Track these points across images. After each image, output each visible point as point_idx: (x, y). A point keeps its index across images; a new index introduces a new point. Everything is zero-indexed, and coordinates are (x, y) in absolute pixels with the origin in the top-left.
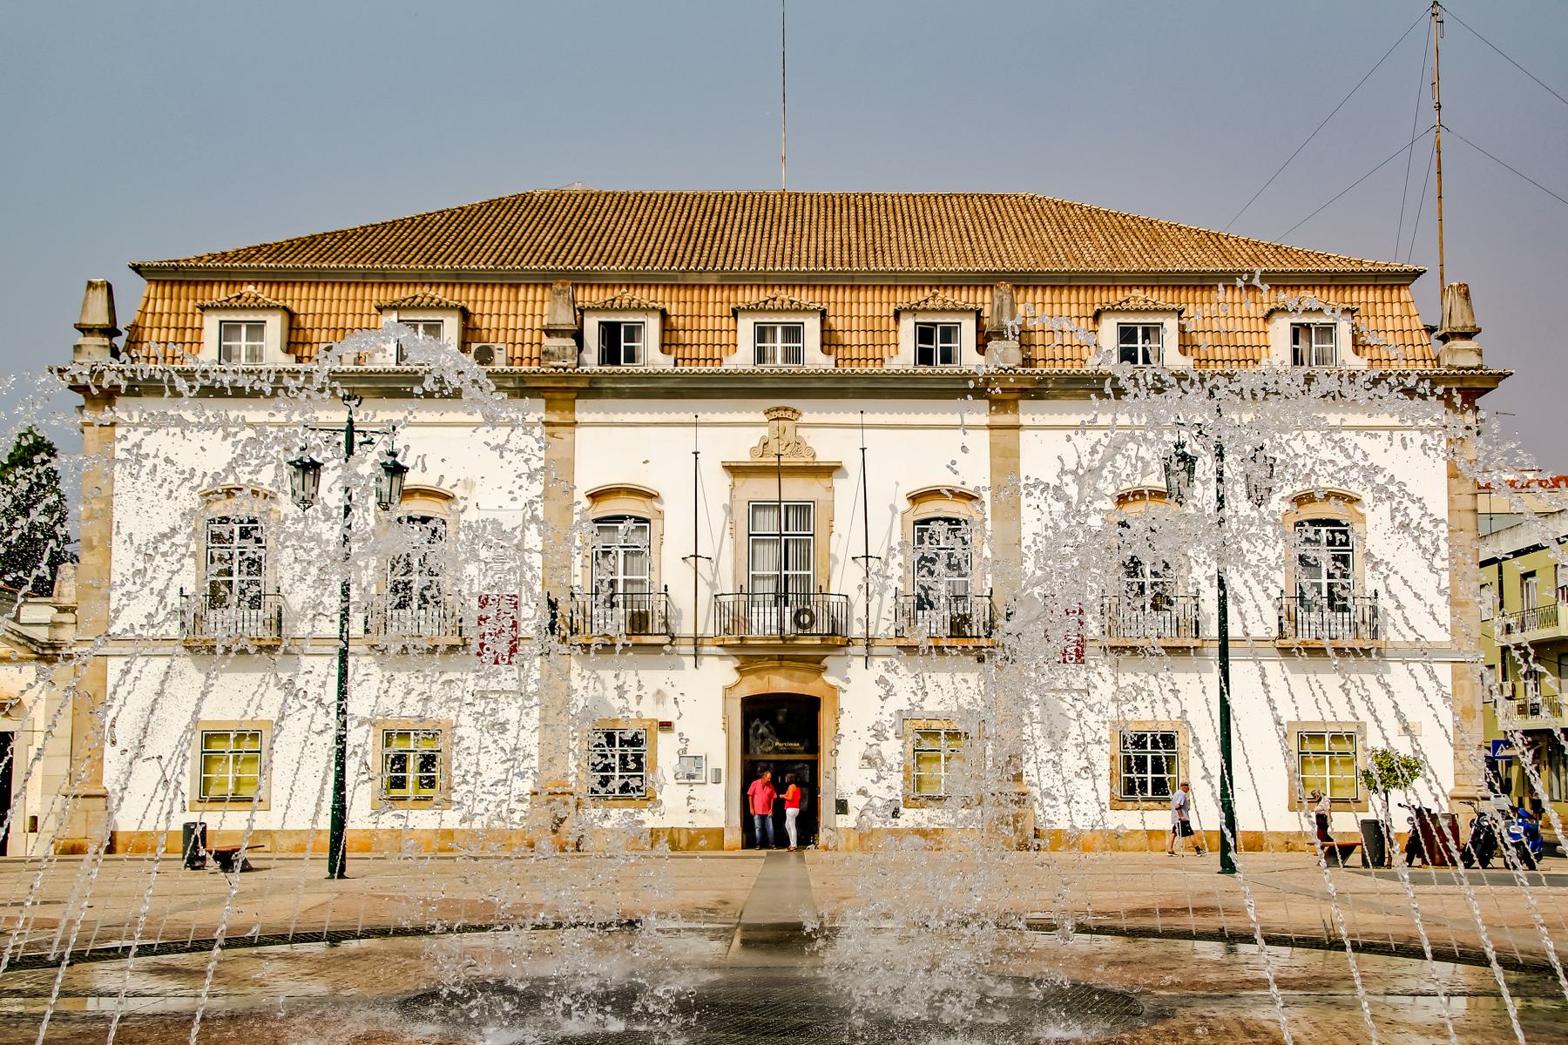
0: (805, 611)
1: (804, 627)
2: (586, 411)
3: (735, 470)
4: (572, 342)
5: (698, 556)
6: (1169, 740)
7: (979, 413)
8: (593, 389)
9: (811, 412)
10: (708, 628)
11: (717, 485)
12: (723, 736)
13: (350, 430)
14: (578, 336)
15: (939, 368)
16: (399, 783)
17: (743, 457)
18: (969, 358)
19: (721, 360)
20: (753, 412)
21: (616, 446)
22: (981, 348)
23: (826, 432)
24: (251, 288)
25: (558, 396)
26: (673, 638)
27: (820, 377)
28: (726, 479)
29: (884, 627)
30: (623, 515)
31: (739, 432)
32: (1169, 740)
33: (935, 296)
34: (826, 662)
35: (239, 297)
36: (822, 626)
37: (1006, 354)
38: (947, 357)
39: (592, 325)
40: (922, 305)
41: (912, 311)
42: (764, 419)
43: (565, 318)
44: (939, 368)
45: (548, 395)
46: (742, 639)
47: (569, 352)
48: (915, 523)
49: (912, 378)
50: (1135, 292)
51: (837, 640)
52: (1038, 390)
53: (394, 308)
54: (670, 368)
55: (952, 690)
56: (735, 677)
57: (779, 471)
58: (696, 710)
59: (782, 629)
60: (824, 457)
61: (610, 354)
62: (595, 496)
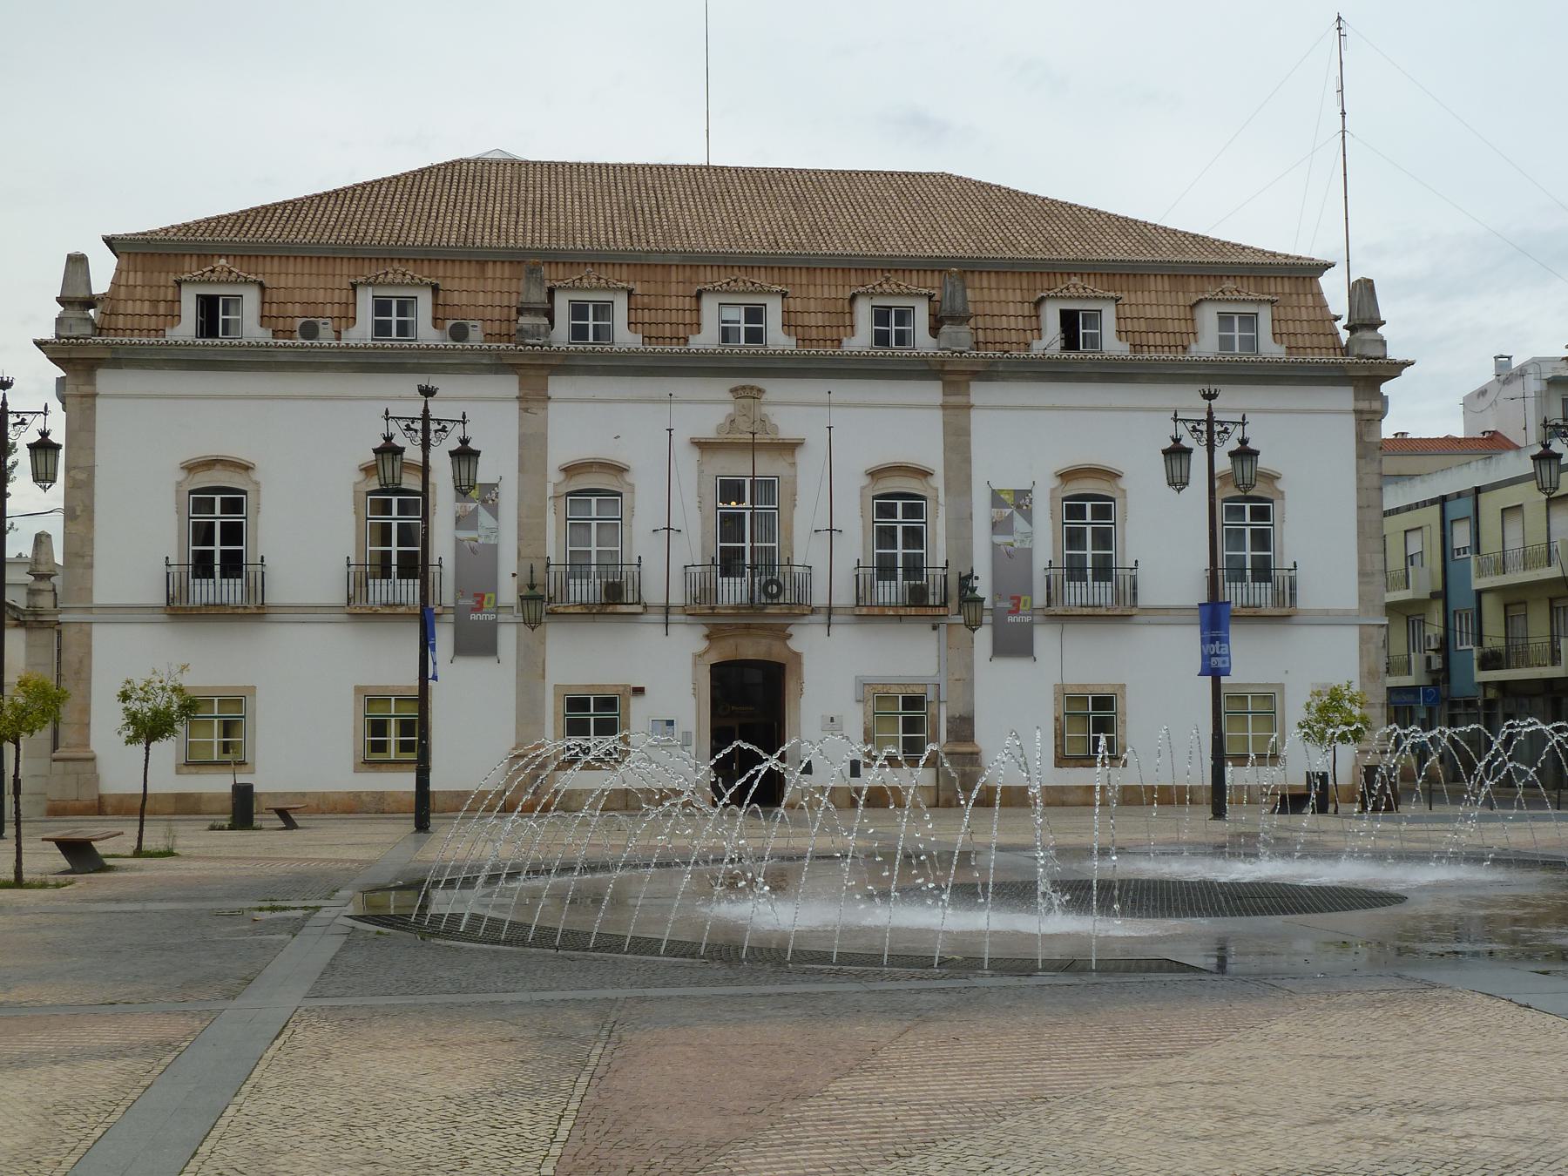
0: (771, 582)
1: (772, 596)
2: (559, 387)
3: (702, 445)
4: (546, 321)
5: (666, 531)
6: (1268, 698)
7: (932, 392)
8: (566, 366)
9: (775, 389)
10: (677, 598)
11: (688, 460)
12: (693, 702)
13: (1210, 421)
14: (550, 314)
15: (894, 350)
16: (379, 747)
17: (708, 432)
18: (923, 341)
19: (840, 341)
20: (720, 388)
21: (590, 420)
22: (934, 331)
23: (791, 408)
24: (223, 261)
25: (532, 373)
26: (645, 607)
27: (783, 356)
28: (695, 454)
29: (844, 596)
30: (596, 489)
31: (706, 408)
32: (1268, 698)
33: (887, 280)
34: (790, 630)
35: (212, 271)
36: (787, 597)
37: (959, 336)
38: (902, 338)
39: (562, 304)
40: (879, 290)
41: (870, 295)
42: (730, 396)
43: (537, 296)
44: (894, 350)
45: (948, 377)
46: (713, 608)
47: (542, 329)
48: (874, 498)
49: (873, 359)
50: (1075, 280)
51: (801, 610)
52: (988, 373)
53: (370, 284)
54: (1284, 357)
55: (911, 657)
56: (704, 644)
57: (753, 447)
58: (666, 675)
59: (752, 599)
60: (787, 432)
61: (1070, 338)
62: (570, 470)
